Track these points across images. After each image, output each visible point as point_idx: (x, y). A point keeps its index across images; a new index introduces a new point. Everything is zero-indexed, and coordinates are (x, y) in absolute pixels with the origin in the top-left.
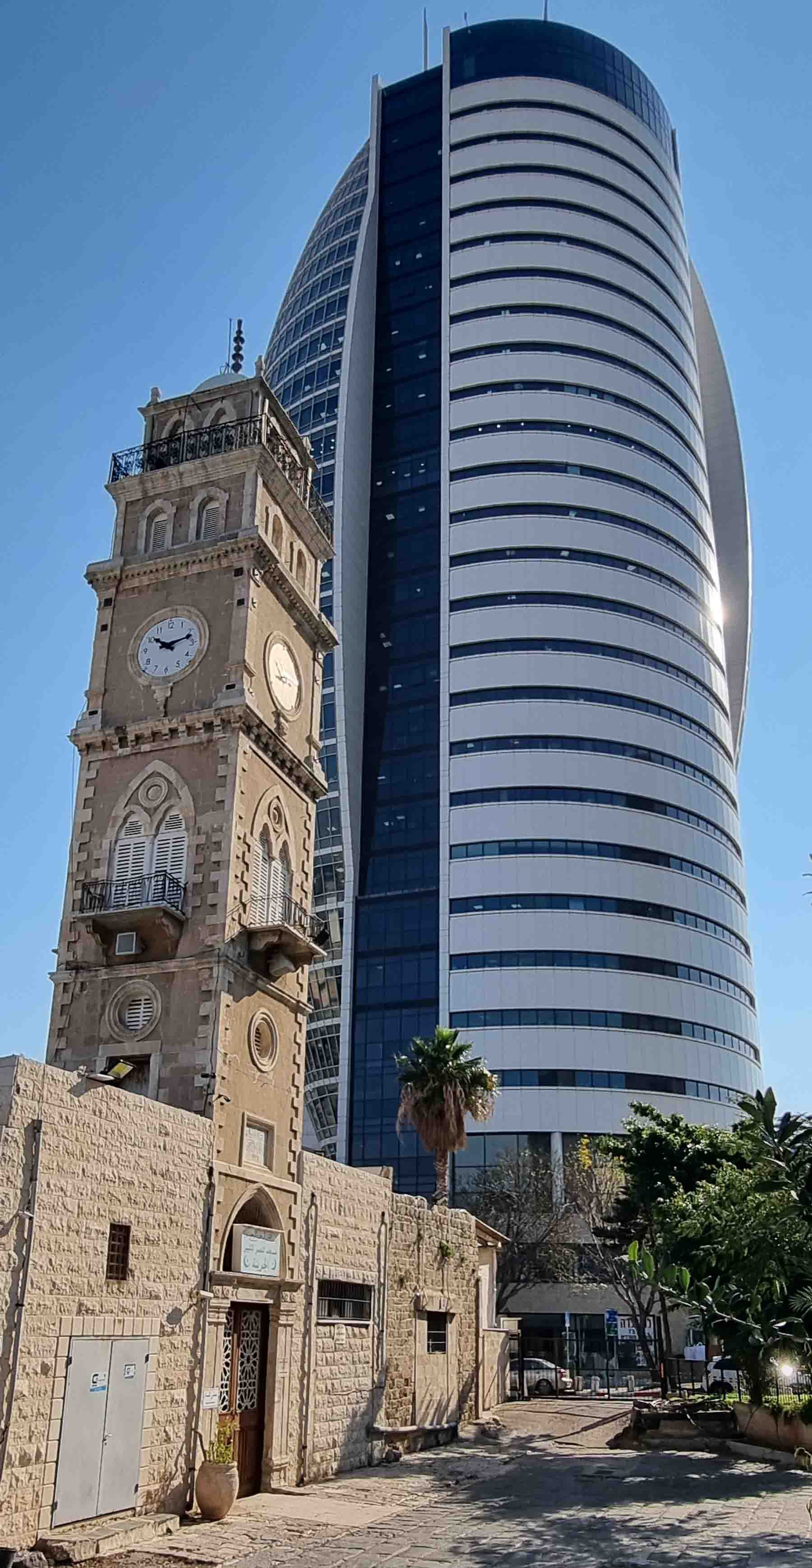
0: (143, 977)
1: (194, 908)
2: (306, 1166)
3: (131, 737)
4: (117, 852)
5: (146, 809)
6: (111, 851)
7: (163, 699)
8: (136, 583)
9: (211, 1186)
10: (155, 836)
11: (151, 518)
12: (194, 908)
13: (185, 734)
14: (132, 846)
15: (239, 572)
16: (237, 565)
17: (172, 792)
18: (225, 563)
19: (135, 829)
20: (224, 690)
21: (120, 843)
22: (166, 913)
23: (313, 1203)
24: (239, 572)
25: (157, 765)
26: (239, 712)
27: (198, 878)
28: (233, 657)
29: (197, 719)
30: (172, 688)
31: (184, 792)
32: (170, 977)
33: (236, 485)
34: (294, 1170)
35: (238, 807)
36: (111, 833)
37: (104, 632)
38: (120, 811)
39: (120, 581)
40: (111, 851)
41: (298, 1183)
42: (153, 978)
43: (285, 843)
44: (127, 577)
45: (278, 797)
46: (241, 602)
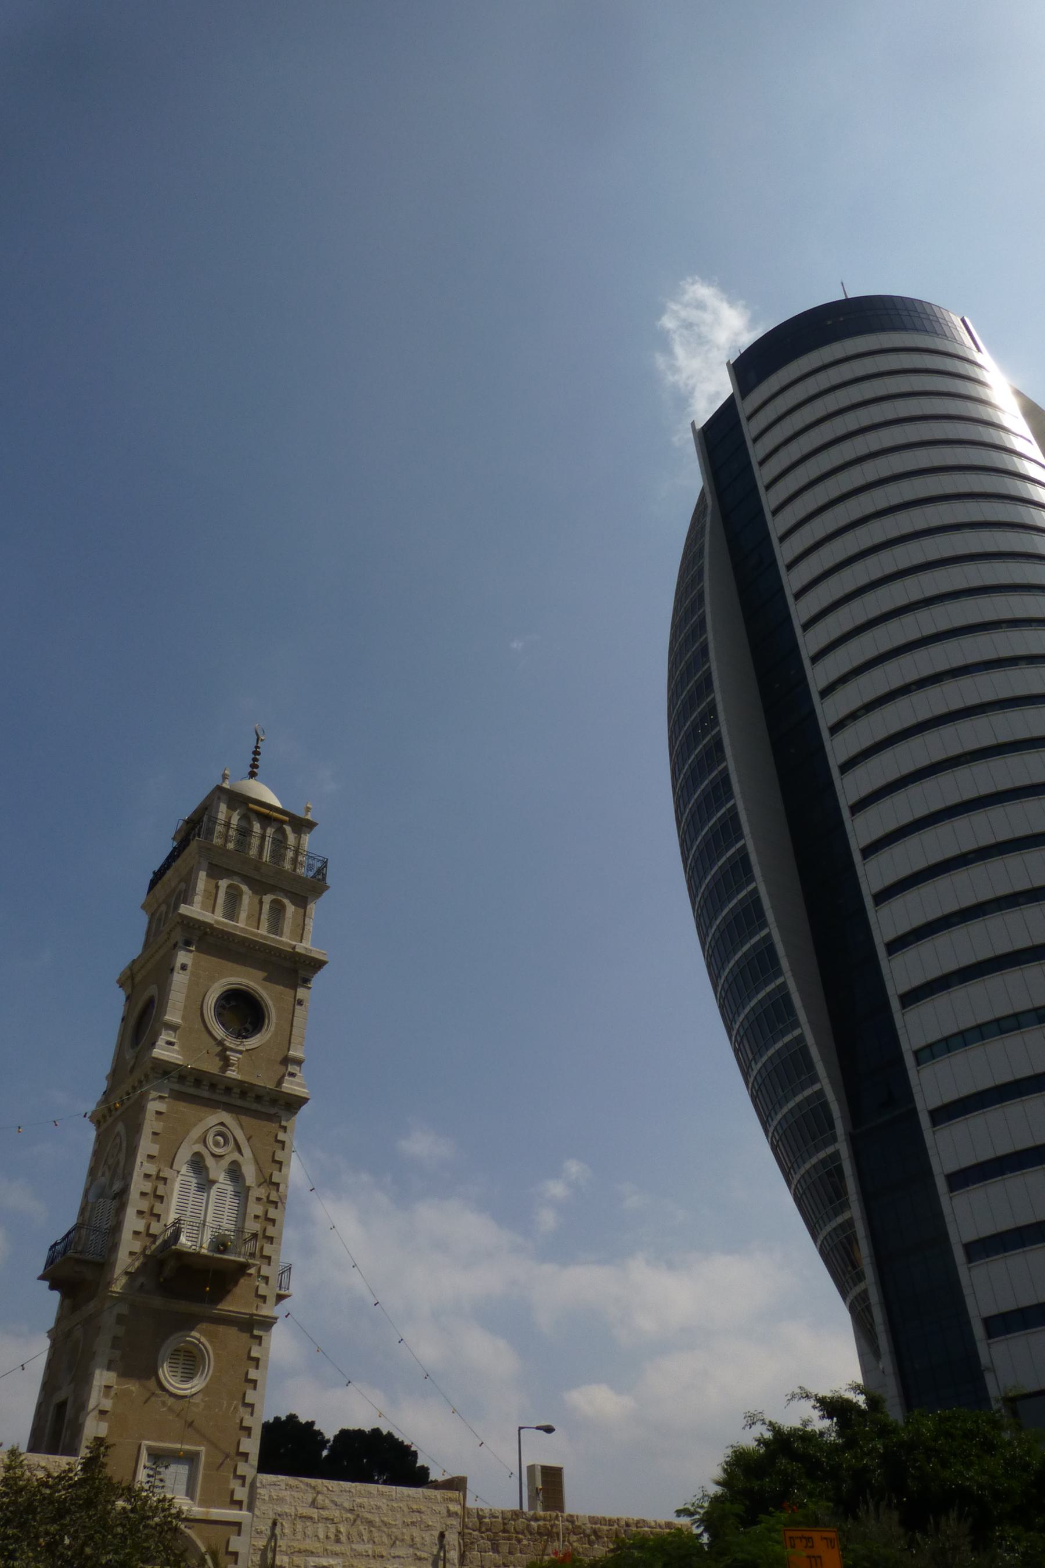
2: (259, 1491)
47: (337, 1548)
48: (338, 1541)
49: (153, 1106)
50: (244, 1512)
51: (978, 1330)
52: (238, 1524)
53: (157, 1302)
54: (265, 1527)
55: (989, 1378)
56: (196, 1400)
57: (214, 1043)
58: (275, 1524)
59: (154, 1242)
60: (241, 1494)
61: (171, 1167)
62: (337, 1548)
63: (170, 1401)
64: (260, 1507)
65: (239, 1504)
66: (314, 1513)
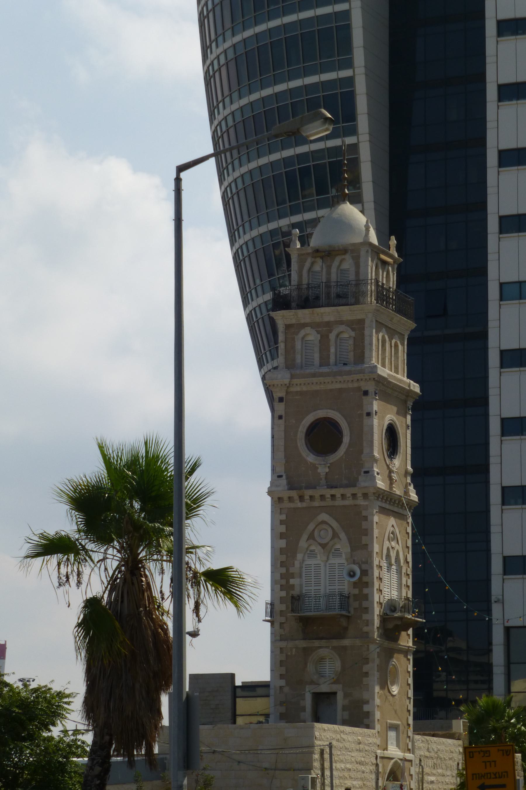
0: (327, 647)
1: (355, 609)
3: (307, 497)
4: (304, 569)
5: (321, 545)
6: (301, 568)
7: (325, 474)
8: (298, 389)
9: (377, 765)
10: (327, 561)
11: (303, 338)
12: (355, 609)
13: (341, 499)
14: (313, 566)
15: (366, 393)
16: (364, 389)
17: (335, 535)
18: (356, 385)
19: (312, 554)
20: (362, 473)
21: (307, 562)
22: (342, 615)
23: (420, 765)
24: (366, 393)
25: (324, 517)
26: (372, 490)
27: (356, 591)
28: (366, 451)
29: (348, 492)
30: (329, 467)
31: (343, 535)
32: (345, 648)
33: (358, 326)
34: (410, 747)
35: (376, 548)
36: (299, 556)
37: (281, 421)
38: (303, 543)
39: (288, 387)
40: (301, 568)
41: (413, 754)
42: (334, 648)
43: (398, 552)
44: (293, 385)
45: (393, 526)
46: (369, 414)
47: (434, 772)
48: (434, 769)
49: (376, 519)
50: (412, 755)
51: (497, 565)
52: (411, 761)
53: (386, 644)
54: (418, 762)
55: (496, 609)
56: (396, 697)
57: (386, 467)
58: (420, 760)
59: (381, 608)
60: (410, 747)
61: (382, 559)
62: (434, 772)
63: (390, 698)
64: (418, 753)
65: (409, 750)
66: (427, 754)
